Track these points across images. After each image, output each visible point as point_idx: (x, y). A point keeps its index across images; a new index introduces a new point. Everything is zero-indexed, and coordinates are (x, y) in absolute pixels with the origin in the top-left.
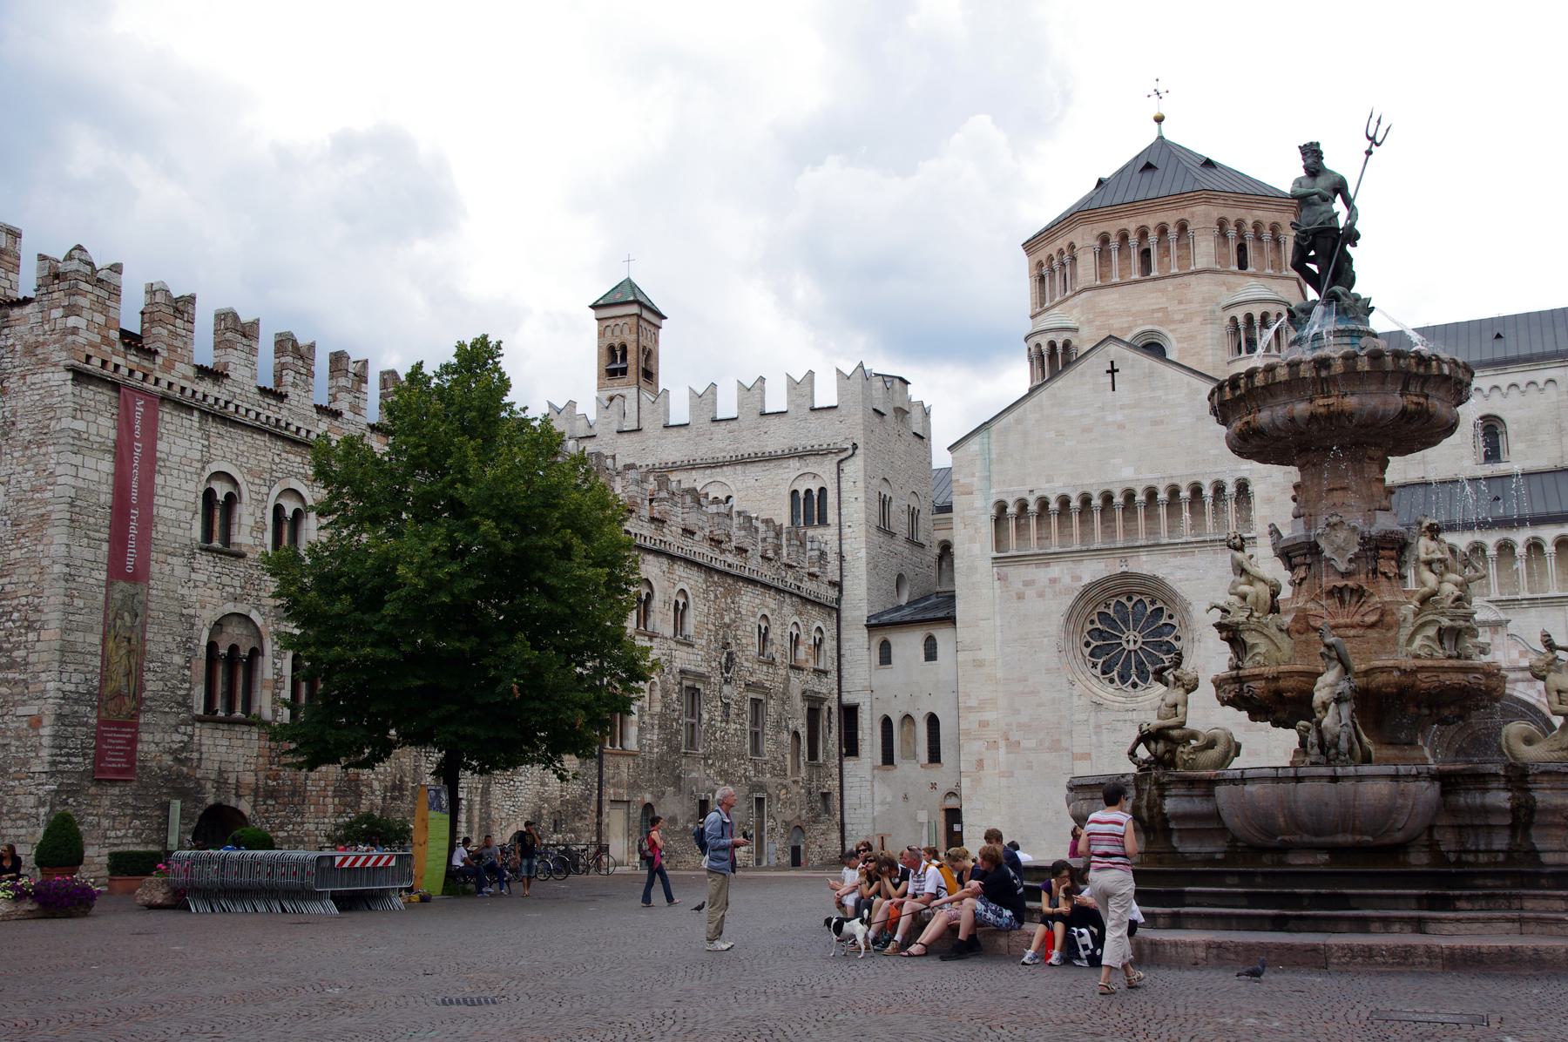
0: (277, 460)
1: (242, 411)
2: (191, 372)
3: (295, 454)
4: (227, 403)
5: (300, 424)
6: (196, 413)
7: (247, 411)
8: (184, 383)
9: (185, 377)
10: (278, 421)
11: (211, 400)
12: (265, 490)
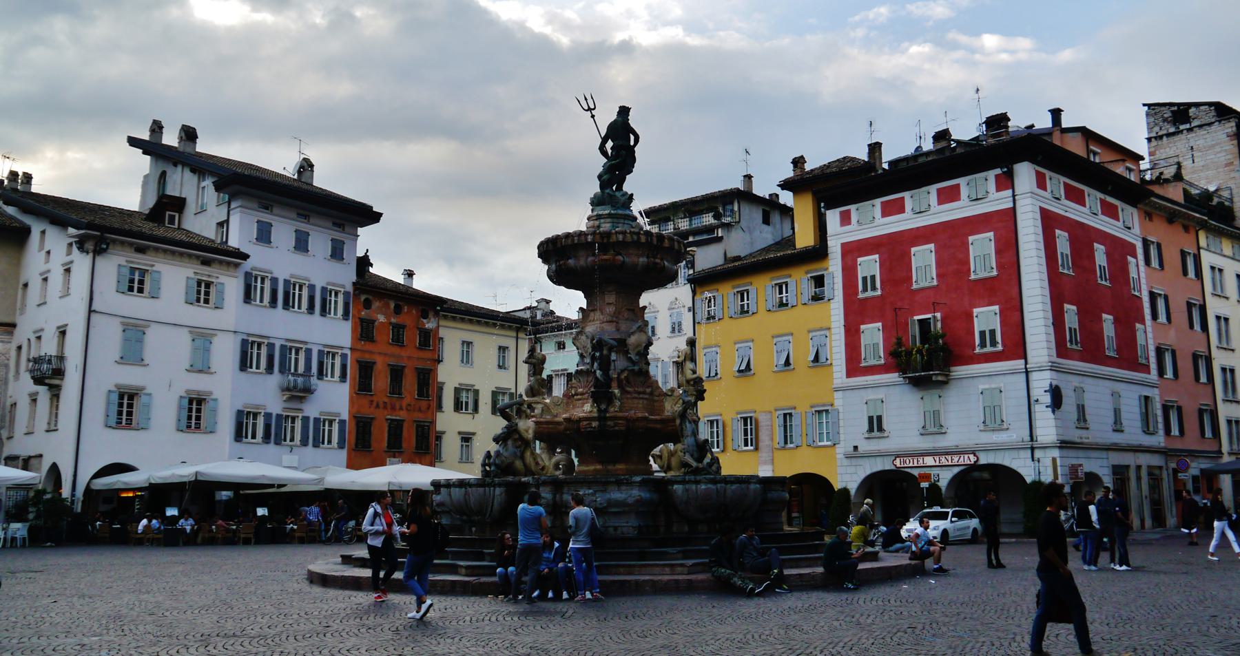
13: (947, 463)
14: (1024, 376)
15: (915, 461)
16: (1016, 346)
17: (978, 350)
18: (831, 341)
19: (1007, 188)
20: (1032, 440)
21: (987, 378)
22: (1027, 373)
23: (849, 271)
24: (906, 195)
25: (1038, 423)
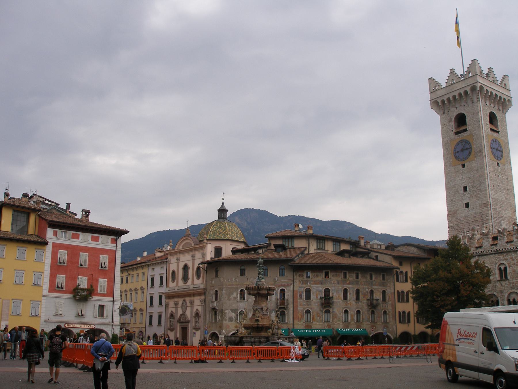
0: (496, 258)
1: (487, 251)
2: (475, 249)
3: (501, 255)
4: (484, 251)
5: (502, 248)
6: (477, 257)
7: (489, 251)
8: (474, 252)
9: (474, 250)
10: (497, 250)
11: (480, 252)
12: (495, 266)
13: (84, 327)
14: (112, 303)
15: (73, 326)
16: (111, 293)
17: (98, 292)
18: (43, 277)
19: (114, 243)
20: (112, 323)
21: (101, 302)
22: (113, 302)
23: (54, 254)
24: (80, 233)
25: (115, 318)
